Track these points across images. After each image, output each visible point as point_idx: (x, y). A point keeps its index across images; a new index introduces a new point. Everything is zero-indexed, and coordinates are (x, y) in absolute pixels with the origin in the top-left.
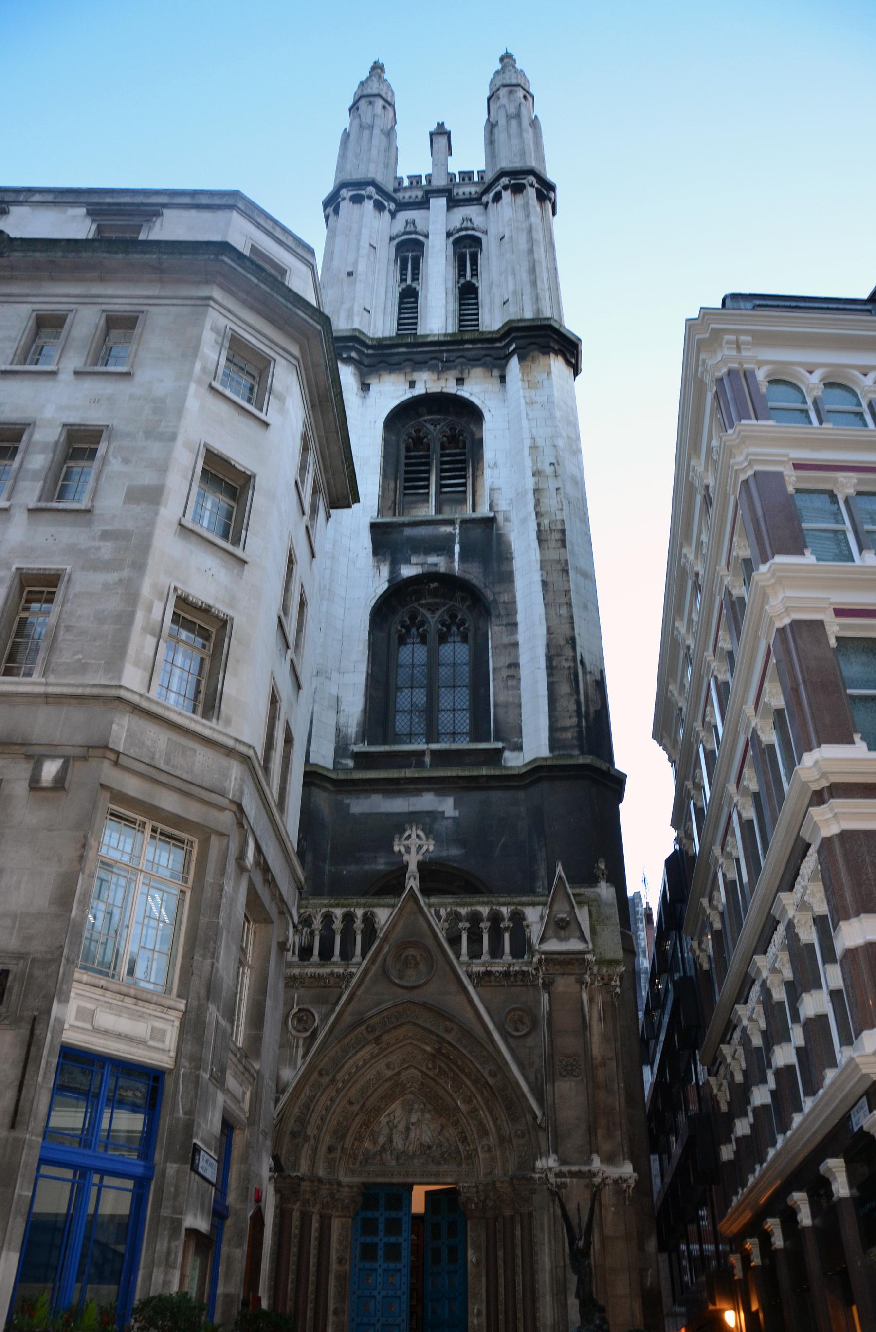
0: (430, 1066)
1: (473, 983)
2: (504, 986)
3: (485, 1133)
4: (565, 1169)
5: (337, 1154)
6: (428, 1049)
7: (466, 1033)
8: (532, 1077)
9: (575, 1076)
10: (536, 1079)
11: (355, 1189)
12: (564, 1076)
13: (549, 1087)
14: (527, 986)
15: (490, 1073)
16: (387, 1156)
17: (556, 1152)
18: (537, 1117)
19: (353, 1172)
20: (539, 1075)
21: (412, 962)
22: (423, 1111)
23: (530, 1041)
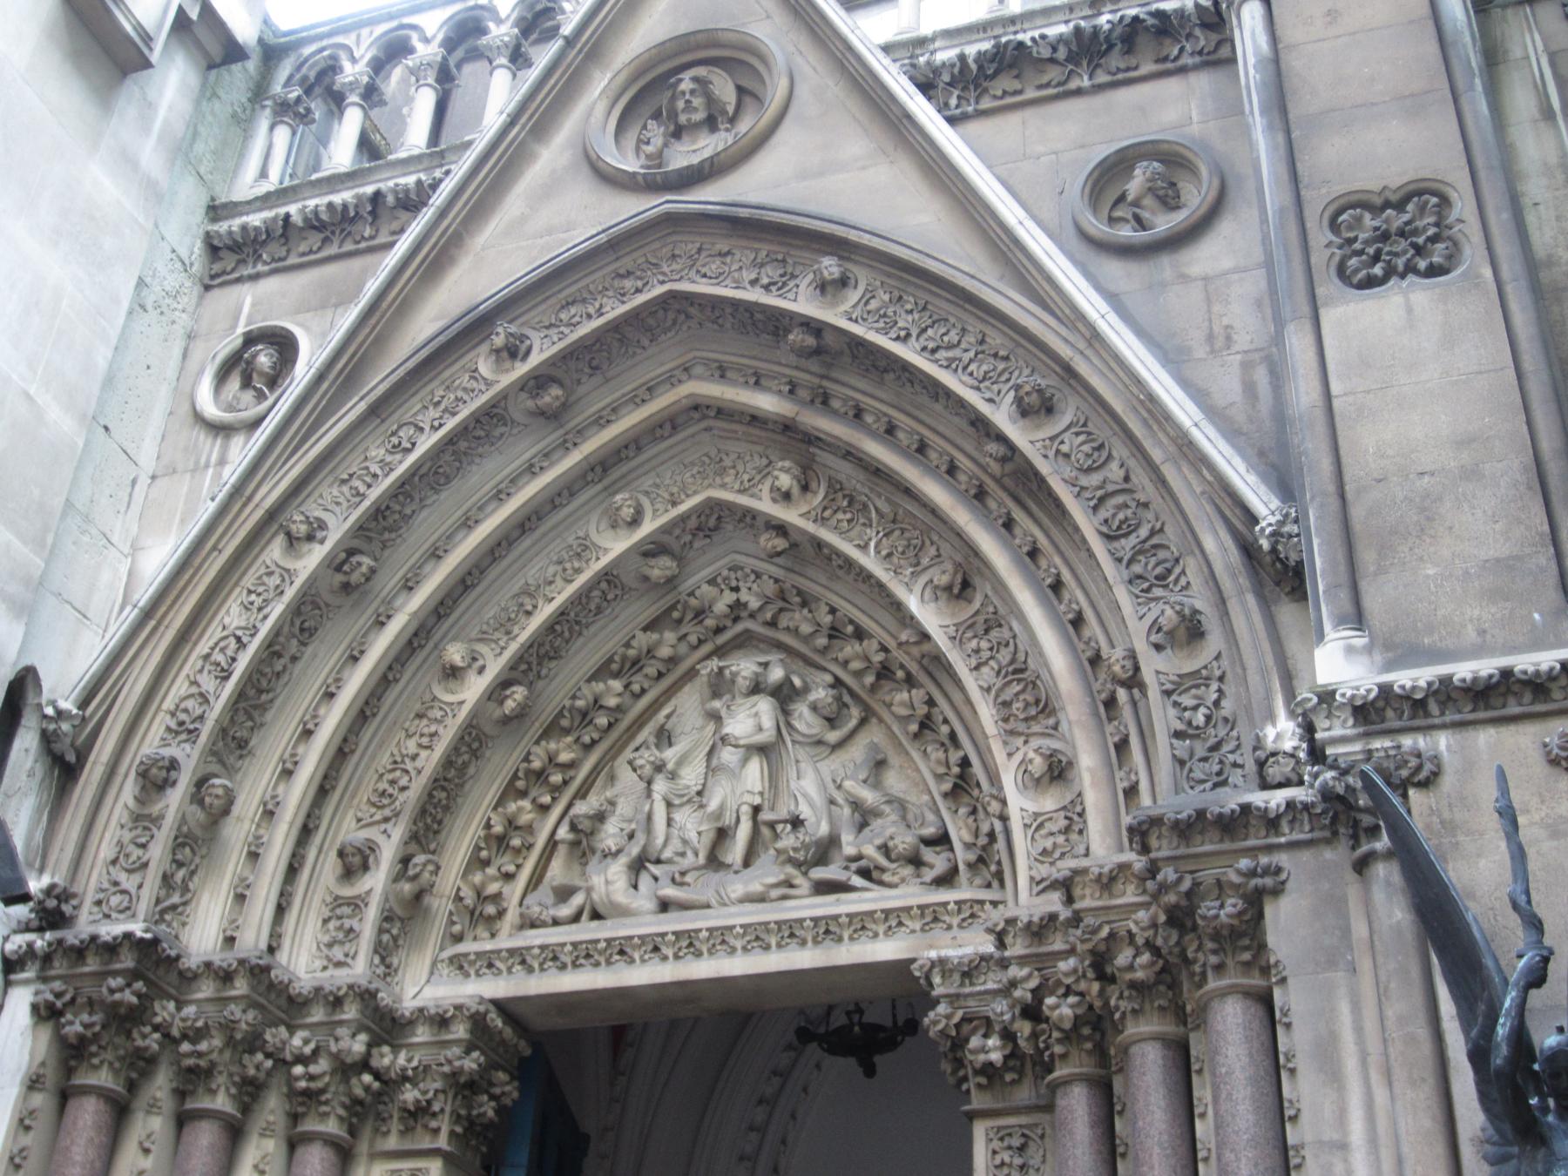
0: (785, 481)
1: (942, 108)
2: (1078, 92)
3: (1031, 704)
4: (1413, 678)
5: (376, 882)
6: (766, 402)
7: (908, 276)
8: (1227, 385)
9: (1434, 271)
10: (1249, 389)
11: (460, 1031)
12: (1370, 283)
13: (1299, 343)
14: (1183, 70)
15: (1024, 411)
16: (609, 881)
17: (1357, 618)
18: (1253, 519)
19: (460, 964)
20: (1261, 376)
21: (697, 102)
22: (784, 695)
23: (1208, 256)
